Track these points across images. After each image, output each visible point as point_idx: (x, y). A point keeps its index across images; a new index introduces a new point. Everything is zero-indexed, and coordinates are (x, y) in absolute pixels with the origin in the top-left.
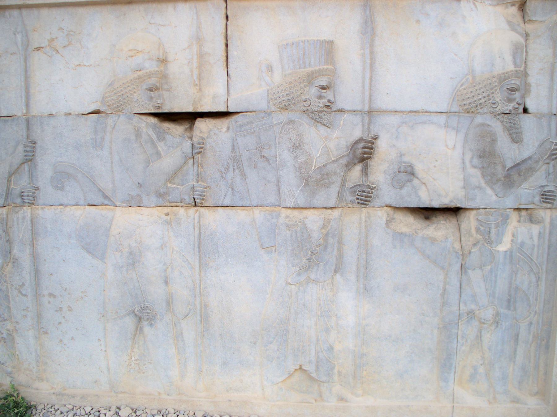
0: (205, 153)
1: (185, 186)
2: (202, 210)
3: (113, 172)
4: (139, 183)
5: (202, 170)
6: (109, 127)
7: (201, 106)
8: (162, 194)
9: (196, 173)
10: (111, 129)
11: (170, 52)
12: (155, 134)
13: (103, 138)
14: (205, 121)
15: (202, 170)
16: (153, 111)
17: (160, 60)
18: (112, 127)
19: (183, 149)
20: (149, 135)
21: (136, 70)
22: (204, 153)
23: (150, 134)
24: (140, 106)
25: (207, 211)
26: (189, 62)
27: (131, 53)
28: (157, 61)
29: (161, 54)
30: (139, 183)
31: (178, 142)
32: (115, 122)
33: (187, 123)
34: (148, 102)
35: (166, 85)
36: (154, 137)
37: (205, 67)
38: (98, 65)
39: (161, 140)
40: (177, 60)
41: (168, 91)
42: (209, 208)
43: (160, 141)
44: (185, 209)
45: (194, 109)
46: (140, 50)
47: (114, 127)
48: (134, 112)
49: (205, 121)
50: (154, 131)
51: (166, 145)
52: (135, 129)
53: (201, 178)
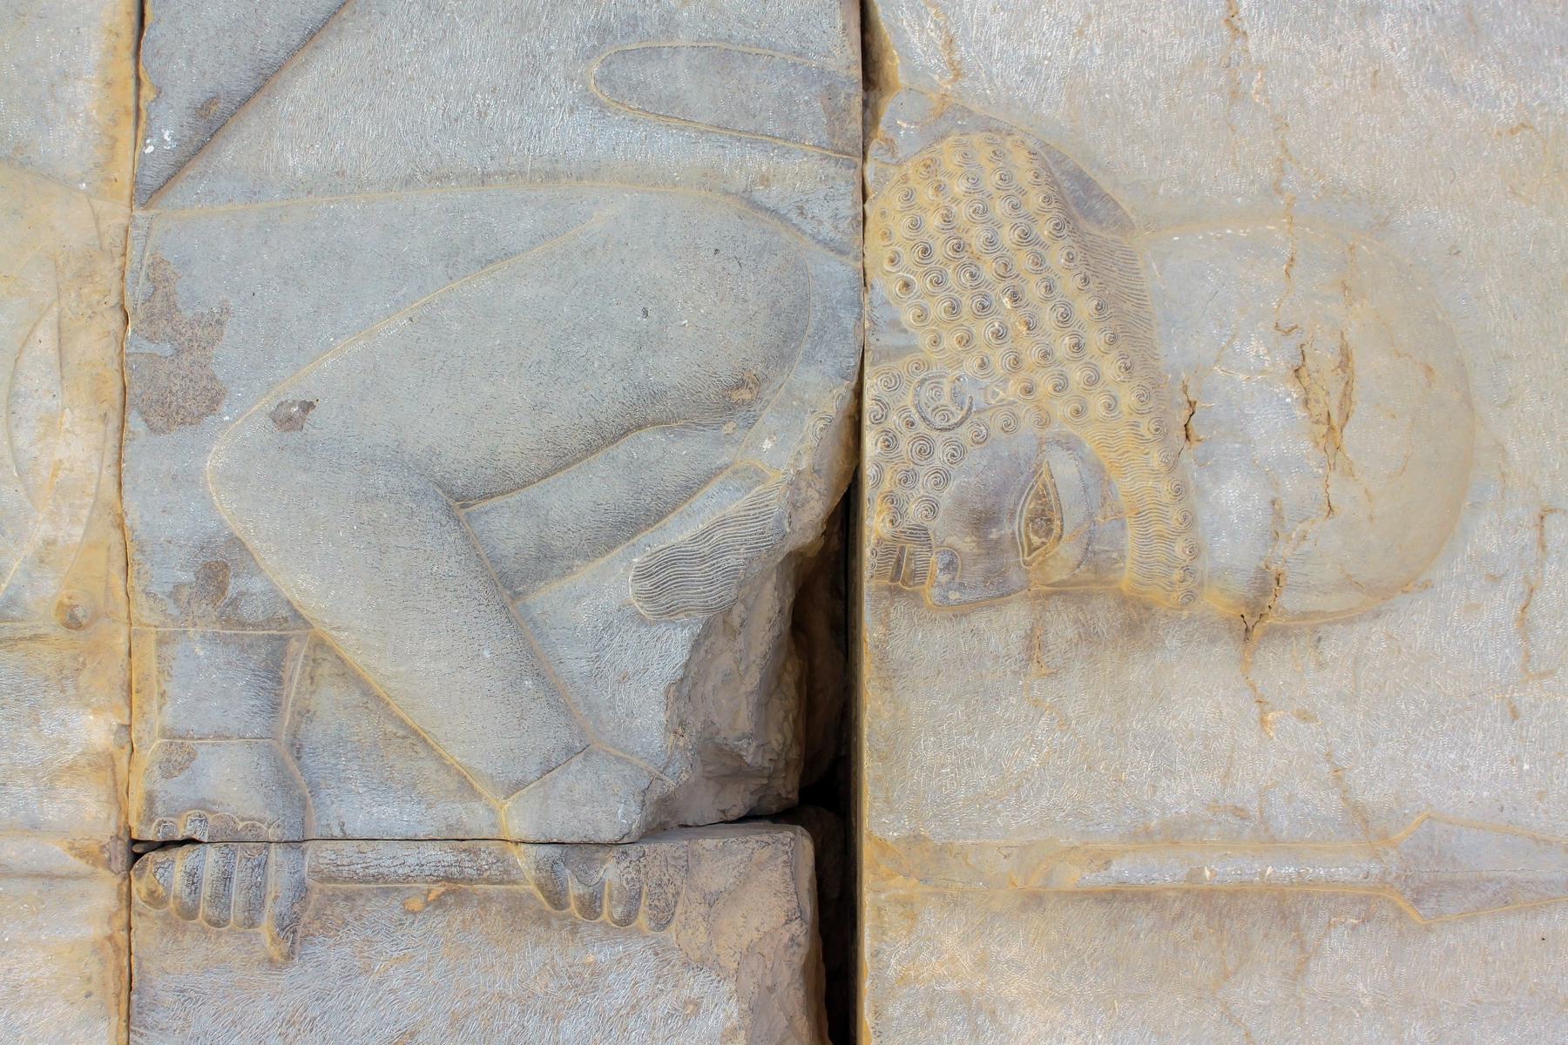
0: (548, 925)
1: (293, 767)
2: (103, 893)
3: (408, 182)
4: (308, 406)
5: (416, 904)
6: (758, 161)
7: (908, 908)
8: (222, 589)
9: (387, 858)
10: (739, 181)
11: (1321, 665)
12: (694, 539)
13: (668, 111)
14: (789, 921)
15: (416, 904)
16: (875, 525)
17: (1264, 591)
18: (760, 194)
19: (576, 764)
20: (689, 490)
21: (1192, 404)
22: (543, 919)
23: (698, 501)
24: (922, 427)
25: (95, 931)
26: (1240, 813)
27: (1324, 357)
28: (1263, 572)
29: (1312, 602)
30: (308, 406)
31: (631, 714)
32: (793, 216)
33: (776, 740)
34: (945, 498)
35: (1071, 633)
36: (678, 532)
37: (1197, 935)
38: (1236, 95)
39: (647, 584)
40: (1263, 721)
41: (1030, 648)
42: (117, 950)
43: (644, 574)
44: (112, 756)
45: (882, 845)
46: (1351, 435)
47: (757, 206)
48: (867, 369)
49: (789, 921)
50: (718, 535)
51: (608, 626)
52: (741, 385)
53: (349, 898)
